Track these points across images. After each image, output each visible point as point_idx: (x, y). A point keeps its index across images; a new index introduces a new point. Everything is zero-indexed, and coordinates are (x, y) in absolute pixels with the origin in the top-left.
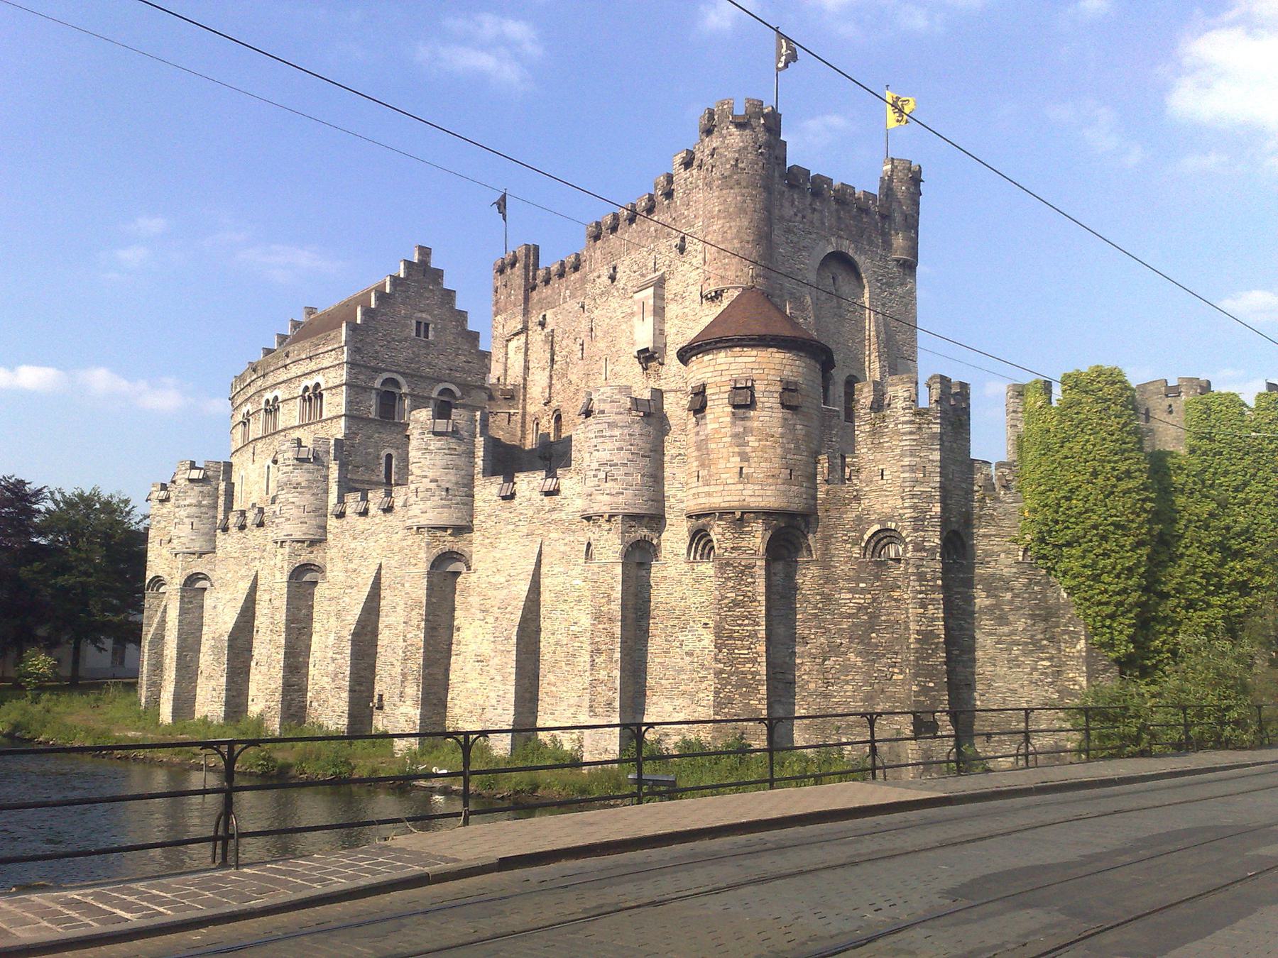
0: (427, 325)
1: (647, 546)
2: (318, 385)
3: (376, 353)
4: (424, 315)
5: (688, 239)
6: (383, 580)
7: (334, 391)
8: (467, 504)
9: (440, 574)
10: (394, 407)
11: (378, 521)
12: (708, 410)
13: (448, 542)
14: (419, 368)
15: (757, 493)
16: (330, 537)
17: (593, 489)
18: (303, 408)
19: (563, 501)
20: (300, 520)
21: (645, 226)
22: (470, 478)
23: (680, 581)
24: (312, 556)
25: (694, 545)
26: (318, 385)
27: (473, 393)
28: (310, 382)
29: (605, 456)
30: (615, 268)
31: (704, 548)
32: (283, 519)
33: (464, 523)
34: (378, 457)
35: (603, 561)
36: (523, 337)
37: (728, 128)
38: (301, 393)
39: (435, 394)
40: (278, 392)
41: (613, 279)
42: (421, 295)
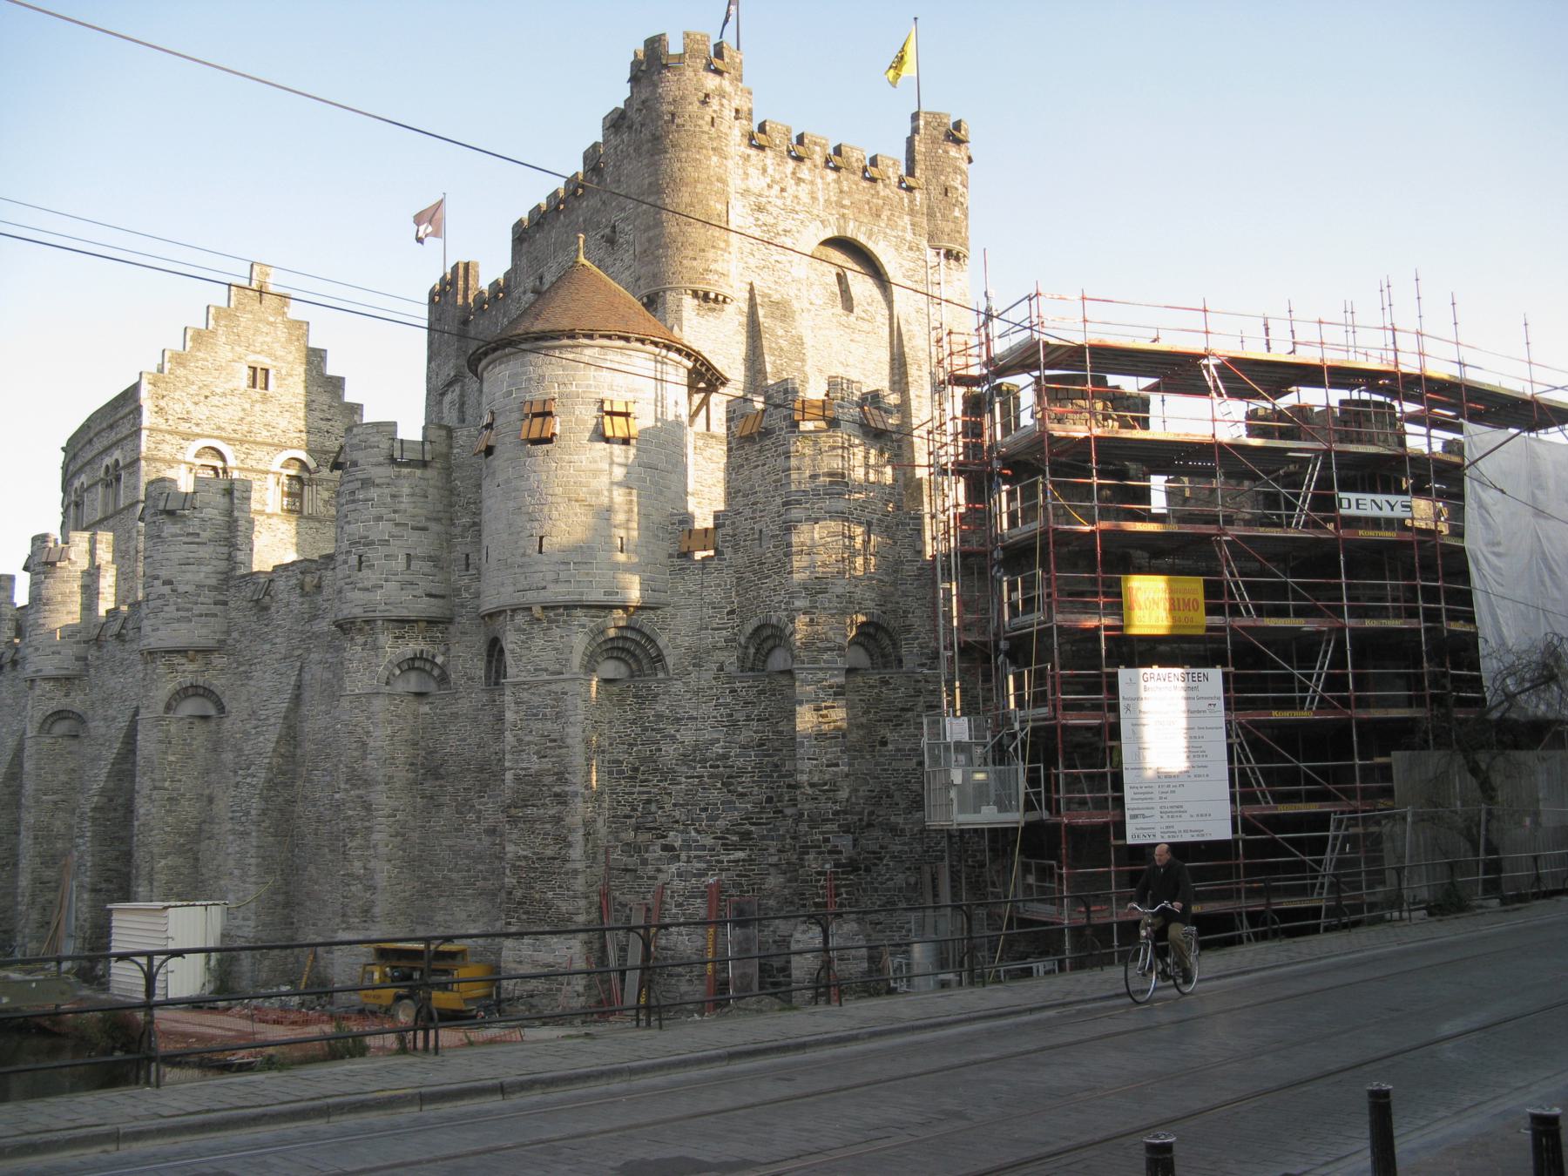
0: (267, 371)
1: (428, 667)
2: (117, 461)
3: (188, 413)
8: (215, 615)
9: (182, 719)
12: (496, 452)
13: (188, 672)
15: (563, 576)
16: (92, 671)
17: (342, 583)
18: (105, 496)
21: (573, 217)
23: (475, 720)
25: (494, 663)
26: (117, 461)
28: (108, 461)
32: (31, 649)
33: (211, 643)
36: (457, 388)
38: (102, 473)
40: (83, 478)
42: (257, 330)
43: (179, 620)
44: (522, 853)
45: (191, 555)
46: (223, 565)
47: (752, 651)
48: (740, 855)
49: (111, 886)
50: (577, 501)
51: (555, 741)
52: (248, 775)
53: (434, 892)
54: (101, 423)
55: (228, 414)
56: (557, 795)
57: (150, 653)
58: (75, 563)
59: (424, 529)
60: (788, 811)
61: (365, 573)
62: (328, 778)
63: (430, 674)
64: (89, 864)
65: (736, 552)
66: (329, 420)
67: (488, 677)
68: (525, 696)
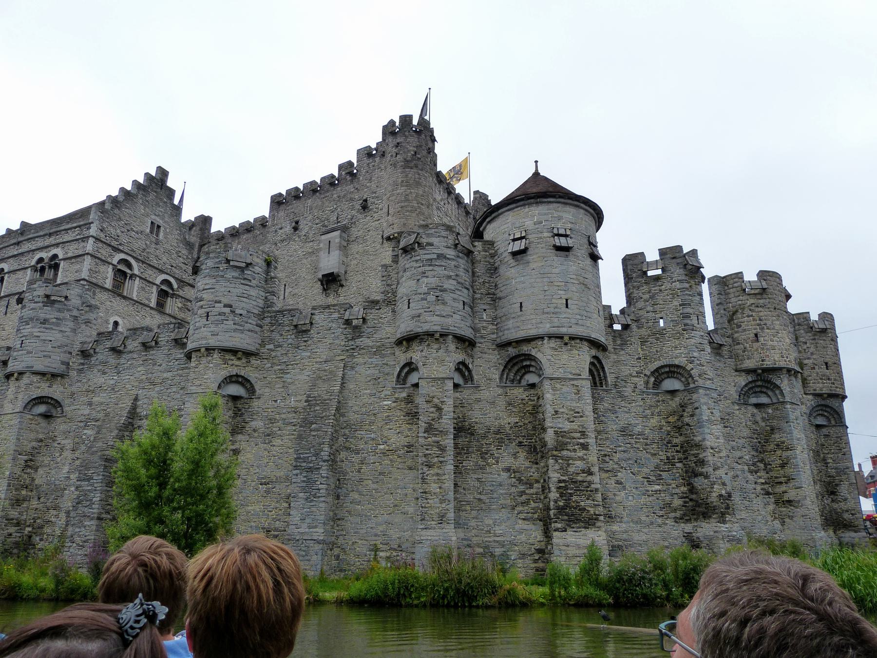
0: (159, 227)
3: (118, 236)
4: (158, 220)
5: (370, 201)
6: (138, 410)
7: (73, 260)
8: (257, 333)
9: (224, 396)
10: (124, 284)
11: (135, 356)
12: (528, 253)
14: (148, 258)
15: (580, 322)
16: (73, 374)
17: (422, 311)
19: (371, 330)
20: (45, 353)
22: (261, 310)
24: (51, 390)
26: (55, 256)
27: (187, 288)
28: (45, 255)
29: (433, 281)
30: (297, 223)
31: (515, 374)
32: (25, 352)
33: (252, 348)
34: (107, 322)
35: (433, 376)
37: (409, 132)
38: (33, 263)
39: (158, 282)
41: (295, 229)
42: (157, 205)
43: (235, 330)
44: (564, 478)
45: (245, 292)
46: (261, 303)
47: (652, 379)
48: (657, 487)
49: (109, 517)
50: (583, 284)
51: (578, 413)
52: (311, 431)
53: (468, 508)
54: (37, 232)
55: (138, 245)
56: (582, 444)
57: (207, 349)
58: (70, 300)
59: (468, 289)
60: (679, 465)
61: (441, 307)
62: (373, 436)
63: (463, 375)
64: (98, 499)
65: (639, 328)
66: (187, 265)
67: (501, 378)
68: (558, 386)
